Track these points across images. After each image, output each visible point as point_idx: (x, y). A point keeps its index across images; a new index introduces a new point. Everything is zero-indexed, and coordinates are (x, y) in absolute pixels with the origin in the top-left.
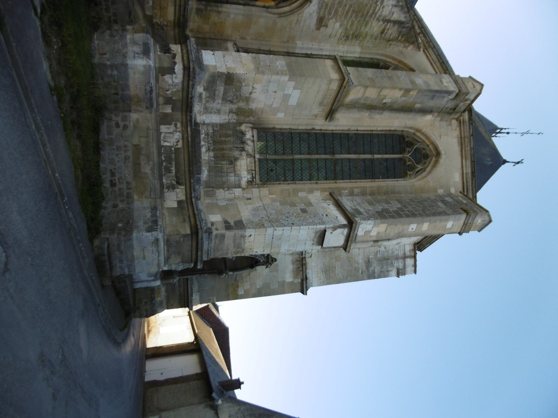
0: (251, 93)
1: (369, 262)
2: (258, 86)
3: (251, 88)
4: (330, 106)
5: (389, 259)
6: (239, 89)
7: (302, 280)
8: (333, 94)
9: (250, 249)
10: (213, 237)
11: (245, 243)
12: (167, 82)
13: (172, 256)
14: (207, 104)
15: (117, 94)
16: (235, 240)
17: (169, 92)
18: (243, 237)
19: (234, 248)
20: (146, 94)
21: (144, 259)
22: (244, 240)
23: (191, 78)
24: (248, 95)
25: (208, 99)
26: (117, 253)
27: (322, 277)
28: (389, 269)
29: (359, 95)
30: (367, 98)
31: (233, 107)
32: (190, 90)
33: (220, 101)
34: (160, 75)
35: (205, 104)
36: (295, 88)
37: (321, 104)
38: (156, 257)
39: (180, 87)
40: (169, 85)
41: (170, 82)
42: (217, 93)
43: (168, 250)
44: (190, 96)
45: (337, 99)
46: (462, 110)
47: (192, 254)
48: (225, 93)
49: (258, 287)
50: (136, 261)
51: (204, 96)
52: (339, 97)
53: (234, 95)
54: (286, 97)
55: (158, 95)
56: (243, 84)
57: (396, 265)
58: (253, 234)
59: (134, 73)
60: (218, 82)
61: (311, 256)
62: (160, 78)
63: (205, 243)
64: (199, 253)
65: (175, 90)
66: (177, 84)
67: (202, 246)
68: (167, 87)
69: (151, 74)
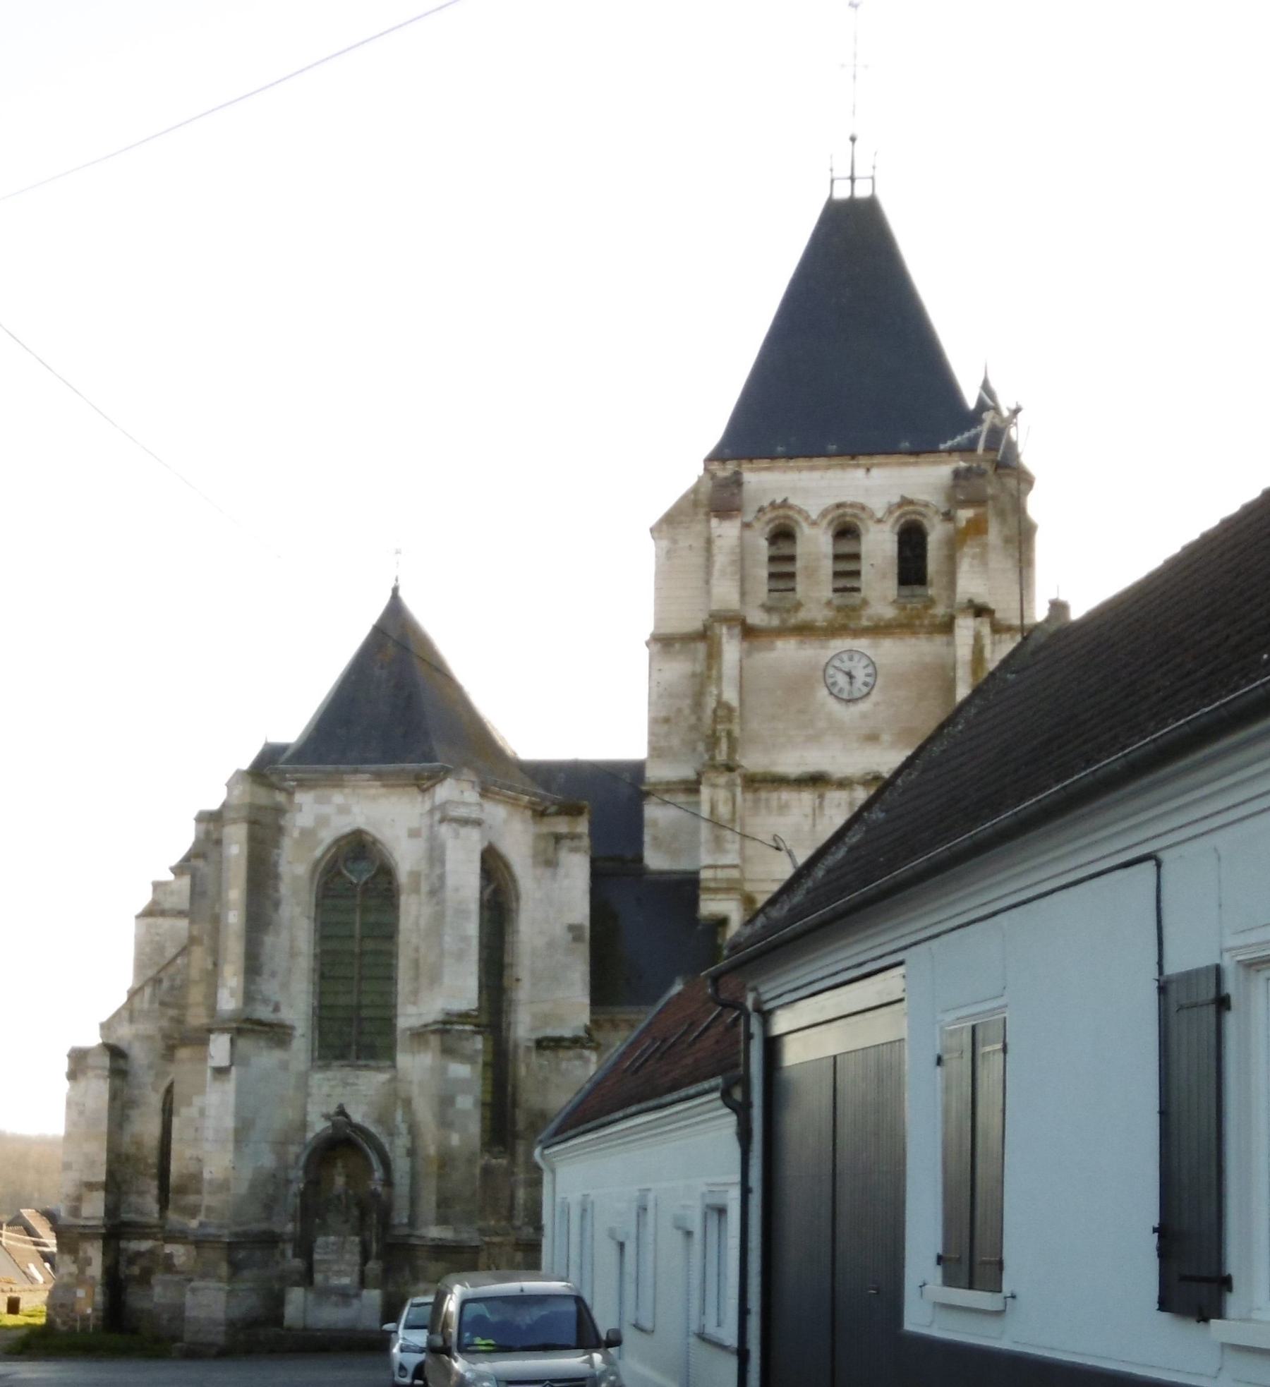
18: (211, 1182)
67: (209, 1235)
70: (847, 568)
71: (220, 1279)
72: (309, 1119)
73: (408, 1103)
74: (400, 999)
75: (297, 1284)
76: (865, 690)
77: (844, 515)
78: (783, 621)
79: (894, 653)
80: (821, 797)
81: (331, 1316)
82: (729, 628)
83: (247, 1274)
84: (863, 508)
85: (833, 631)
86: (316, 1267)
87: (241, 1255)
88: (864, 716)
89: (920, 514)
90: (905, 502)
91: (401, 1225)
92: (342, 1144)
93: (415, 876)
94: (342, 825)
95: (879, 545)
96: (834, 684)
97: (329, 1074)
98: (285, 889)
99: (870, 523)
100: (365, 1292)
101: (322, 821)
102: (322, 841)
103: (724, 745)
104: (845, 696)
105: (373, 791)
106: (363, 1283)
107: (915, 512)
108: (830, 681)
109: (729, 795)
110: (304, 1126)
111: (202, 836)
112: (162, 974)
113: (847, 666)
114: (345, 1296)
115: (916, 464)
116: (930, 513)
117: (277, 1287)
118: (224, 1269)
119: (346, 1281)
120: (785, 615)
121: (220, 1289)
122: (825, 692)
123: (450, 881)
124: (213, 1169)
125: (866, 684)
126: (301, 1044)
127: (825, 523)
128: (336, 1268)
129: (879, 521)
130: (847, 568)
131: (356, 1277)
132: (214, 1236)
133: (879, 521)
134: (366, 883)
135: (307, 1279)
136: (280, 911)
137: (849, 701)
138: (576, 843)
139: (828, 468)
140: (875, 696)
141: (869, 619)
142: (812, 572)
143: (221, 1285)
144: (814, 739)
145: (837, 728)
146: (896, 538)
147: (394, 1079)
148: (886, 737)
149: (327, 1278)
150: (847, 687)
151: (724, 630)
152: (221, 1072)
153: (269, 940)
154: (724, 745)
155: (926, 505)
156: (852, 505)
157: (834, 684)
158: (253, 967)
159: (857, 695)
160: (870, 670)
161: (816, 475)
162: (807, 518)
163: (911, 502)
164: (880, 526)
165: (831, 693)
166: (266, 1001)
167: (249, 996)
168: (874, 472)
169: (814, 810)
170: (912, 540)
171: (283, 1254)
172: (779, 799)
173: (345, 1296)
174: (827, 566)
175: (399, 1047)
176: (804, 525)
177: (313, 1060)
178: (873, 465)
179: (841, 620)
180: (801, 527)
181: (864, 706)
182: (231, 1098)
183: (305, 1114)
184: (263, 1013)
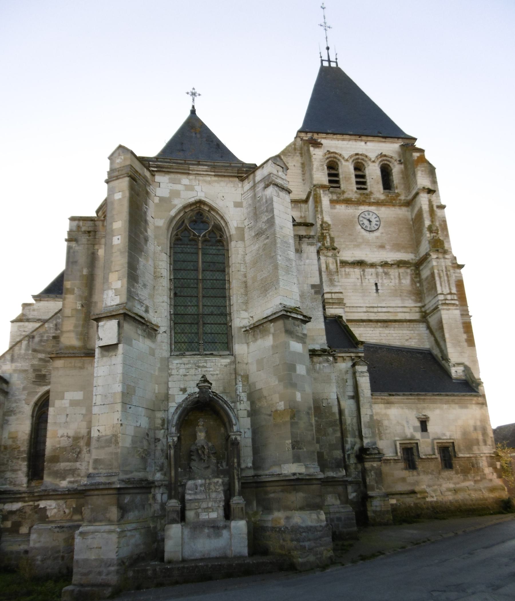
0: (69, 437)
1: (257, 234)
2: (60, 432)
3: (62, 438)
4: (83, 359)
5: (255, 207)
6: (64, 449)
7: (271, 321)
8: (69, 360)
9: (113, 427)
10: (96, 471)
11: (106, 436)
12: (56, 513)
13: (108, 515)
14: (82, 475)
15: (63, 558)
16: (103, 447)
17: (67, 511)
18: (99, 438)
19: (111, 446)
20: (63, 531)
21: (100, 548)
22: (103, 436)
23: (46, 493)
24: (70, 439)
25: (75, 475)
26: (91, 576)
27: (270, 294)
28: (264, 200)
29: (73, 335)
30: (76, 326)
31: (85, 450)
32: (60, 493)
33: (78, 464)
34: (47, 520)
35: (82, 477)
36: (63, 398)
37: (82, 368)
38: (99, 535)
39: (61, 502)
40: (59, 511)
41: (55, 510)
42: (68, 468)
43: (101, 521)
44: (67, 492)
45: (73, 355)
46: (93, 222)
47: (108, 494)
48: (69, 461)
49: (277, 383)
50: (102, 557)
51: (72, 479)
52: (70, 355)
53: (71, 452)
54: (74, 403)
55: (71, 520)
56: (58, 446)
57: (260, 195)
58: (96, 428)
59: (39, 542)
60: (55, 469)
61: (252, 317)
62: (50, 519)
63: (98, 481)
64: (101, 487)
65: (64, 506)
66: (58, 505)
67: (99, 484)
68: (62, 513)
69: (43, 527)
70: (361, 180)
71: (110, 522)
72: (170, 392)
73: (246, 377)
74: (235, 308)
76: (377, 227)
77: (358, 159)
78: (338, 197)
79: (387, 213)
80: (364, 271)
81: (206, 546)
82: (323, 191)
83: (131, 516)
84: (366, 156)
85: (359, 203)
86: (188, 506)
87: (127, 499)
88: (377, 238)
89: (388, 161)
90: (381, 155)
91: (247, 468)
92: (205, 407)
93: (241, 230)
94: (190, 197)
95: (373, 172)
96: (363, 224)
97: (185, 360)
98: (150, 232)
99: (370, 163)
100: (233, 524)
101: (176, 194)
102: (176, 205)
103: (328, 240)
104: (368, 229)
105: (208, 179)
106: (228, 514)
107: (387, 160)
108: (361, 223)
109: (334, 261)
110: (167, 398)
111: (74, 229)
112: (35, 333)
113: (368, 217)
115: (385, 142)
116: (393, 161)
118: (114, 513)
120: (338, 195)
121: (110, 532)
122: (360, 227)
123: (277, 221)
124: (101, 428)
125: (377, 225)
126: (163, 337)
127: (351, 161)
129: (374, 162)
130: (361, 180)
132: (105, 484)
133: (374, 162)
134: (204, 236)
135: (182, 518)
136: (148, 245)
137: (370, 231)
138: (311, 240)
139: (350, 140)
140: (381, 230)
141: (374, 199)
142: (348, 179)
143: (112, 527)
144: (358, 246)
145: (367, 243)
146: (379, 170)
147: (234, 362)
148: (388, 247)
150: (369, 226)
151: (322, 192)
152: (108, 349)
153: (142, 261)
154: (328, 240)
155: (391, 157)
156: (361, 155)
157: (363, 224)
158: (133, 275)
159: (374, 229)
160: (377, 219)
161: (345, 142)
162: (343, 158)
163: (385, 156)
164: (374, 164)
165: (362, 228)
166: (141, 302)
167: (131, 295)
168: (368, 143)
169: (361, 276)
170: (386, 172)
172: (345, 271)
173: (215, 528)
174: (354, 180)
175: (235, 340)
176: (342, 161)
177: (171, 351)
178: (368, 141)
179: (362, 198)
180: (341, 162)
181: (376, 234)
182: (119, 369)
183: (168, 388)
184: (139, 310)
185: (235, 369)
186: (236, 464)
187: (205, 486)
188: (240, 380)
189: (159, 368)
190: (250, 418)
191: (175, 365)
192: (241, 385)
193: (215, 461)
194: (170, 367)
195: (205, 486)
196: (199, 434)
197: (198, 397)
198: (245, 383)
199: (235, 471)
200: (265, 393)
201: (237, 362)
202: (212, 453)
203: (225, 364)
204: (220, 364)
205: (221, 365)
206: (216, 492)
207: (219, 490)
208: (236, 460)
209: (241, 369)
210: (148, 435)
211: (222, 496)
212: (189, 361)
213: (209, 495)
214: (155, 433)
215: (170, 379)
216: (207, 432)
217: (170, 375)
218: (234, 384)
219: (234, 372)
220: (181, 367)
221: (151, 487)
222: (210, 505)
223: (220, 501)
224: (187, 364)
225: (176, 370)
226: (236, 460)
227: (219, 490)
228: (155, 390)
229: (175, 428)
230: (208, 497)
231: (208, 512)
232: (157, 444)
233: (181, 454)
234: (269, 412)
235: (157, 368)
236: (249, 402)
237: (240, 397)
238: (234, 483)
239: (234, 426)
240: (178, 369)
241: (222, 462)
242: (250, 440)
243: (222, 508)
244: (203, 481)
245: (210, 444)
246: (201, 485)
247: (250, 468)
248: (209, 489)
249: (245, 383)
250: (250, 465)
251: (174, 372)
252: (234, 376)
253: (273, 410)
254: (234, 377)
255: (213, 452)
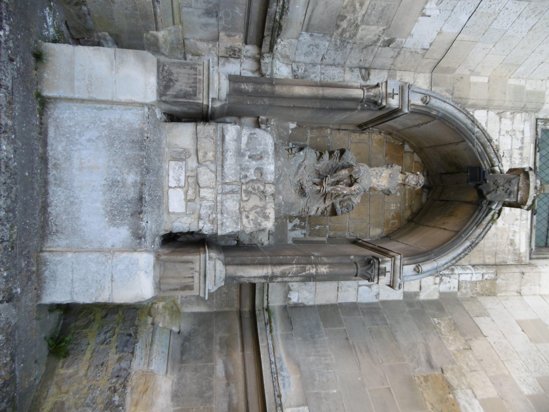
49: (527, 391)
73: (490, 290)
75: (165, 82)
114: (138, 205)
117: (161, 34)
119: (176, 201)
128: (206, 177)
131: (182, 225)
149: (180, 156)
171: (233, 54)
185: (504, 265)
186: (313, 271)
187: (258, 180)
188: (486, 276)
189: (522, 88)
190: (401, 298)
191: (521, 127)
192: (474, 279)
193: (313, 213)
194: (518, 116)
195: (258, 180)
196: (386, 172)
197: (493, 172)
198: (479, 289)
199: (294, 268)
200: (478, 345)
201: (523, 270)
202: (333, 205)
203: (517, 241)
204: (517, 229)
205: (515, 232)
206: (241, 213)
207: (245, 220)
208: (323, 270)
209: (509, 279)
210: (388, 43)
211: (228, 227)
212: (528, 158)
213: (233, 192)
214: (382, 69)
215: (492, 114)
216: (387, 193)
217: (500, 115)
218: (474, 262)
219: (498, 261)
220: (515, 141)
221: (260, 46)
222: (204, 193)
223: (213, 222)
224: (521, 154)
225: (509, 129)
226: (323, 270)
227: (245, 220)
228: (478, 74)
229: (420, 103)
230: (228, 188)
231: (185, 188)
232: (357, 72)
233: (329, 131)
234: (437, 360)
235: (523, 83)
236: (436, 297)
237: (449, 276)
238: (263, 264)
239: (413, 266)
240: (512, 133)
241: (303, 228)
242: (351, 299)
243: (194, 228)
244: (270, 177)
245: (356, 200)
246: (260, 170)
247: (287, 298)
248: (248, 193)
249: (479, 289)
250: (294, 298)
251: (506, 124)
252: (491, 261)
253: (448, 375)
254: (487, 261)
255: (338, 206)
